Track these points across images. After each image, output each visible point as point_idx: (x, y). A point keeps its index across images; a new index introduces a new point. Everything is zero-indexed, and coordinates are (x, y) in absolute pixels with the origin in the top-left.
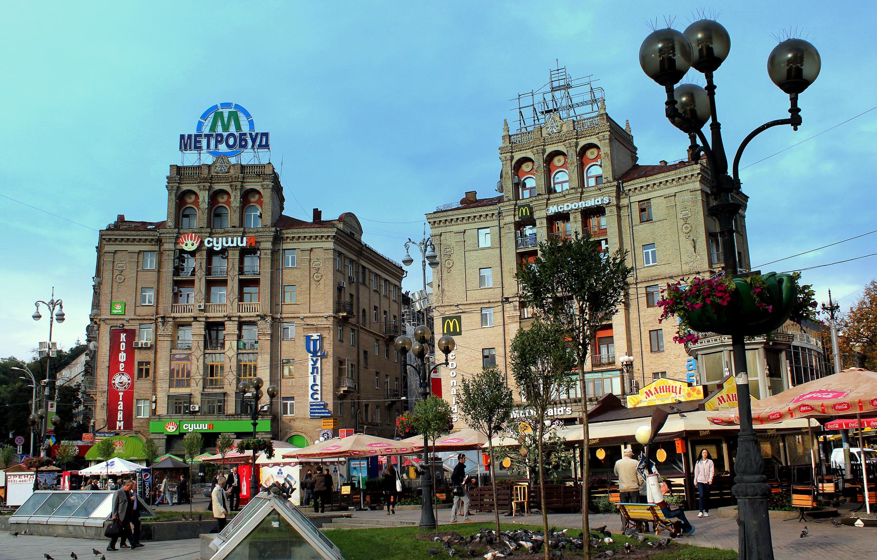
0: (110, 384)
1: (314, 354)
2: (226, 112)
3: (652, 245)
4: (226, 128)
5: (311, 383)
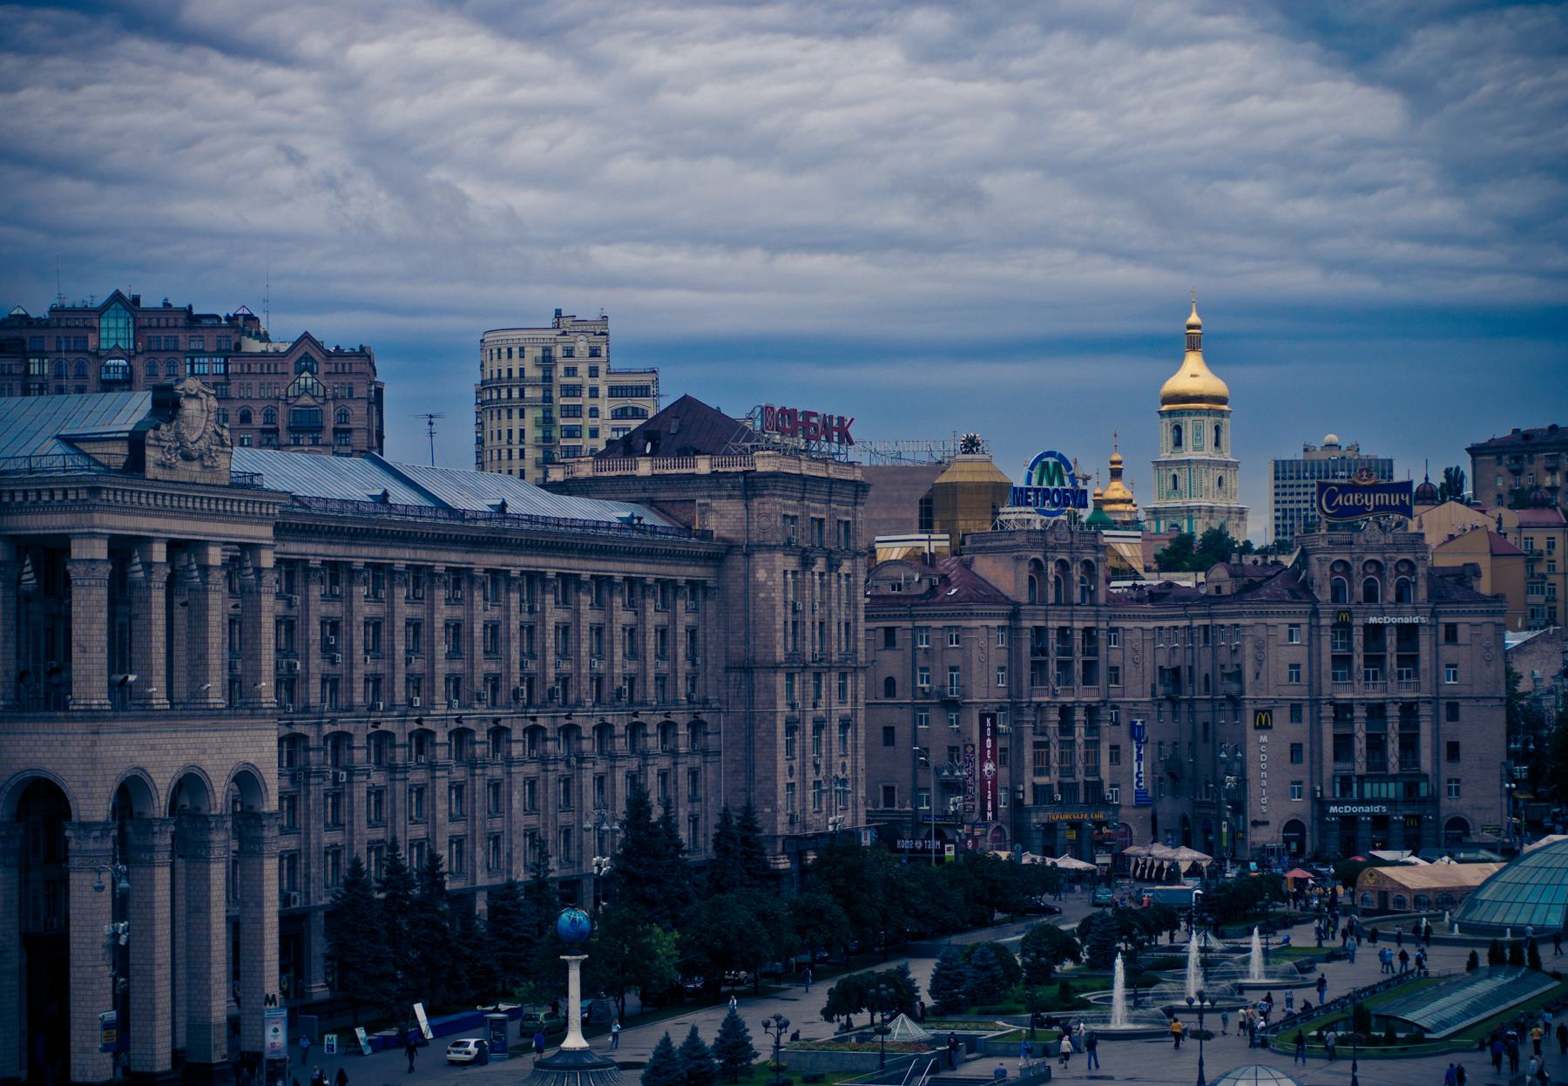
0: (982, 773)
1: (1139, 741)
2: (1051, 460)
4: (1051, 483)
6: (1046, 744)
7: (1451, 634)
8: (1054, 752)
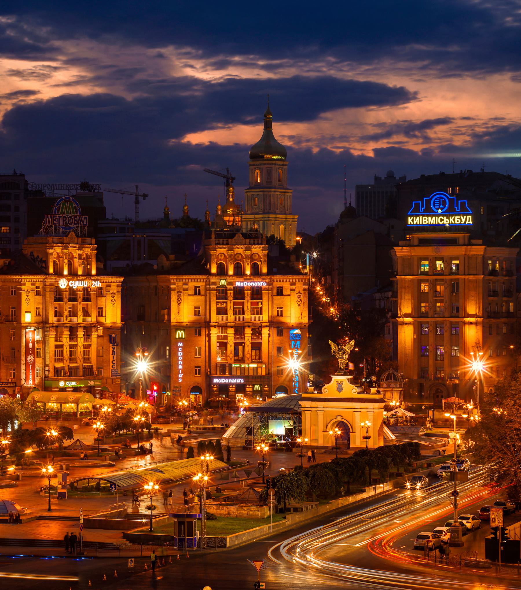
3: (281, 308)
5: (111, 359)
6: (61, 346)
7: (280, 292)
8: (66, 350)
